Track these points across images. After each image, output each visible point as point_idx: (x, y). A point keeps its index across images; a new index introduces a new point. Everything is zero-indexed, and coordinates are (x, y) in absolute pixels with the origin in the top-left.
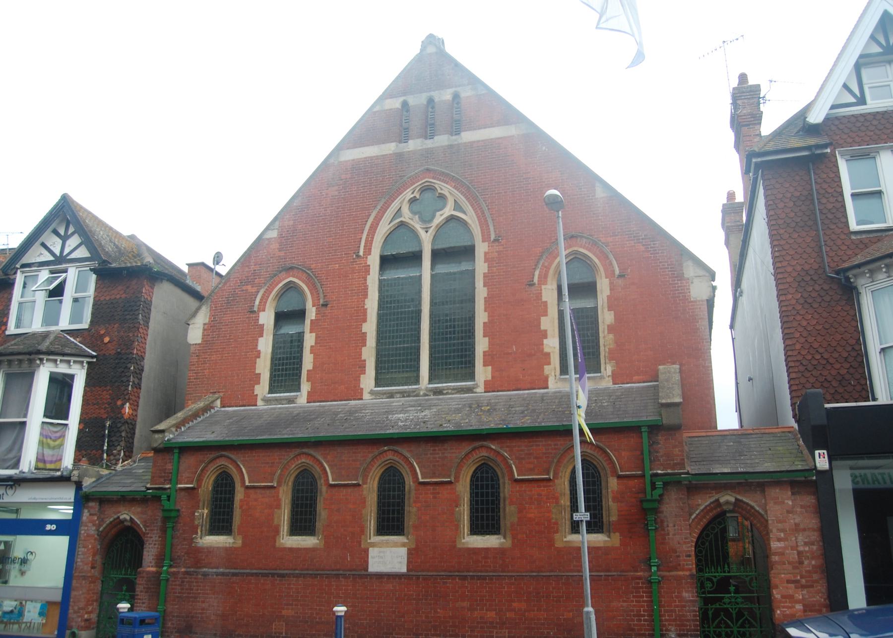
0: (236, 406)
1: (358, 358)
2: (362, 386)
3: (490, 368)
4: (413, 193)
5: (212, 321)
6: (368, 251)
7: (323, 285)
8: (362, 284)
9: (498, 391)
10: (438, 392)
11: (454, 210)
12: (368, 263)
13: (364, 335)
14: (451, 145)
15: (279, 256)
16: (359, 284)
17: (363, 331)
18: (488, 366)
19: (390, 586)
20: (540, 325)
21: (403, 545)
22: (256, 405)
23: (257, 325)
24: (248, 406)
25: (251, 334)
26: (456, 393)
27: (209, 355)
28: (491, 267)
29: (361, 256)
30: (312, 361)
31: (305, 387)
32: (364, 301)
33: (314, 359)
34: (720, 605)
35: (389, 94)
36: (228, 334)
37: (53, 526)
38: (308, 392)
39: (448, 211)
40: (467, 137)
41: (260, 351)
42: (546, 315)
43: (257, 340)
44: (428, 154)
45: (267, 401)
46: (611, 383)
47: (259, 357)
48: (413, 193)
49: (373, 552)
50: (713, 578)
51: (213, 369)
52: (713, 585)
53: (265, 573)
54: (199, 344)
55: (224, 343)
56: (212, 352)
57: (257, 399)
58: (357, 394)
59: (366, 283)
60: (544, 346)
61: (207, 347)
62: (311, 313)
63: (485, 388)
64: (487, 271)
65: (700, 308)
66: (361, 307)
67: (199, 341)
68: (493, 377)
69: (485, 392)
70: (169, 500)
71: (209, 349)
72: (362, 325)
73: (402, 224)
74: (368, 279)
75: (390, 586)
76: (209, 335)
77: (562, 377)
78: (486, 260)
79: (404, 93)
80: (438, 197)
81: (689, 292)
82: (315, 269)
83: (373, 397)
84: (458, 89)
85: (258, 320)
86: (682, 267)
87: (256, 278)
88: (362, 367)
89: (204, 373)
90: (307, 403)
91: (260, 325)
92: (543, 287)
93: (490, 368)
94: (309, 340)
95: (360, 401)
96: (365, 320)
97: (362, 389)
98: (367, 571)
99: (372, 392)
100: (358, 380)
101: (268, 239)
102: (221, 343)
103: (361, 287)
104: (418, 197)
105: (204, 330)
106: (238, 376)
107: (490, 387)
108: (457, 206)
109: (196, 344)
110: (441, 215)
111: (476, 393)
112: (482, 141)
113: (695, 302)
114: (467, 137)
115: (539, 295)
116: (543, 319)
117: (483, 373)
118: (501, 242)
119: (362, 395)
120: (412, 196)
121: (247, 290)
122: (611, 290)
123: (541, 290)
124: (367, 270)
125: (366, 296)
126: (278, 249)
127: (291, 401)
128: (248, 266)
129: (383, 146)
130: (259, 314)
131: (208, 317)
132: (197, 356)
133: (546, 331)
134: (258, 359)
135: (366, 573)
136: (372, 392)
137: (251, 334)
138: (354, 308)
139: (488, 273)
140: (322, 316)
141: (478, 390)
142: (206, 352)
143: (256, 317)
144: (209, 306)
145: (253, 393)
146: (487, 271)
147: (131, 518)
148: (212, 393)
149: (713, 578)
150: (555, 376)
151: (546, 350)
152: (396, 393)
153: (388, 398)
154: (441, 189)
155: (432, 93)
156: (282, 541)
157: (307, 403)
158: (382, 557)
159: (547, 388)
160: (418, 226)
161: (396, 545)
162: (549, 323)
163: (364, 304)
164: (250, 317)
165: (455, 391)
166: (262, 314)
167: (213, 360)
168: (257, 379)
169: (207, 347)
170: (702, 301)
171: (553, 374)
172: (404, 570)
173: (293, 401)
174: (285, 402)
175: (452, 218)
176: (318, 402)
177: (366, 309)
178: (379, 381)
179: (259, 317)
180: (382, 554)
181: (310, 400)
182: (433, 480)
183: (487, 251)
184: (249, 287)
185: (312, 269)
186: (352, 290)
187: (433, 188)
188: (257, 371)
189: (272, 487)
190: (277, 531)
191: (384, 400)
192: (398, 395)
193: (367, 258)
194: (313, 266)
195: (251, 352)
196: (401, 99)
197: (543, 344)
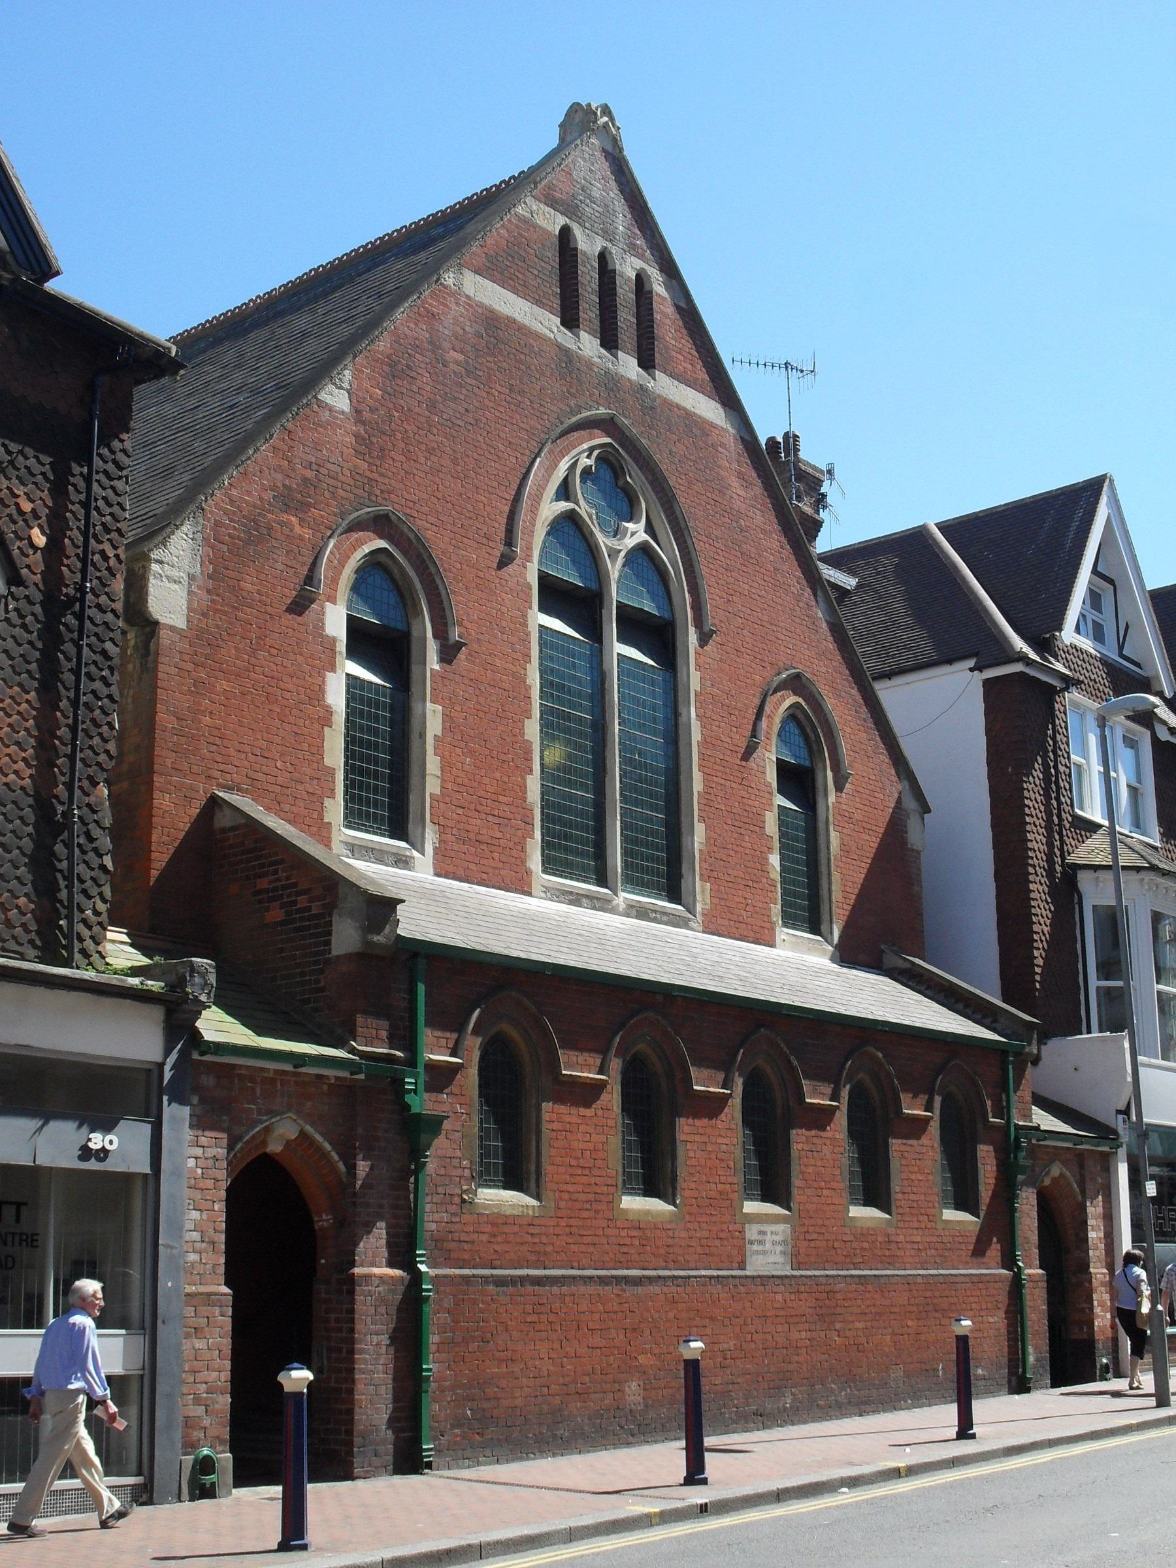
14: (641, 385)
23: (321, 636)
31: (431, 837)
37: (109, 1137)
38: (435, 849)
40: (664, 386)
41: (329, 706)
44: (612, 384)
49: (752, 1232)
53: (607, 1277)
67: (181, 623)
70: (415, 1091)
73: (571, 518)
92: (767, 754)
108: (650, 529)
113: (913, 850)
114: (664, 386)
117: (701, 892)
119: (530, 886)
120: (589, 462)
129: (538, 311)
147: (303, 1134)
161: (776, 1219)
162: (771, 825)
175: (643, 548)
177: (530, 687)
187: (615, 462)
196: (561, 220)
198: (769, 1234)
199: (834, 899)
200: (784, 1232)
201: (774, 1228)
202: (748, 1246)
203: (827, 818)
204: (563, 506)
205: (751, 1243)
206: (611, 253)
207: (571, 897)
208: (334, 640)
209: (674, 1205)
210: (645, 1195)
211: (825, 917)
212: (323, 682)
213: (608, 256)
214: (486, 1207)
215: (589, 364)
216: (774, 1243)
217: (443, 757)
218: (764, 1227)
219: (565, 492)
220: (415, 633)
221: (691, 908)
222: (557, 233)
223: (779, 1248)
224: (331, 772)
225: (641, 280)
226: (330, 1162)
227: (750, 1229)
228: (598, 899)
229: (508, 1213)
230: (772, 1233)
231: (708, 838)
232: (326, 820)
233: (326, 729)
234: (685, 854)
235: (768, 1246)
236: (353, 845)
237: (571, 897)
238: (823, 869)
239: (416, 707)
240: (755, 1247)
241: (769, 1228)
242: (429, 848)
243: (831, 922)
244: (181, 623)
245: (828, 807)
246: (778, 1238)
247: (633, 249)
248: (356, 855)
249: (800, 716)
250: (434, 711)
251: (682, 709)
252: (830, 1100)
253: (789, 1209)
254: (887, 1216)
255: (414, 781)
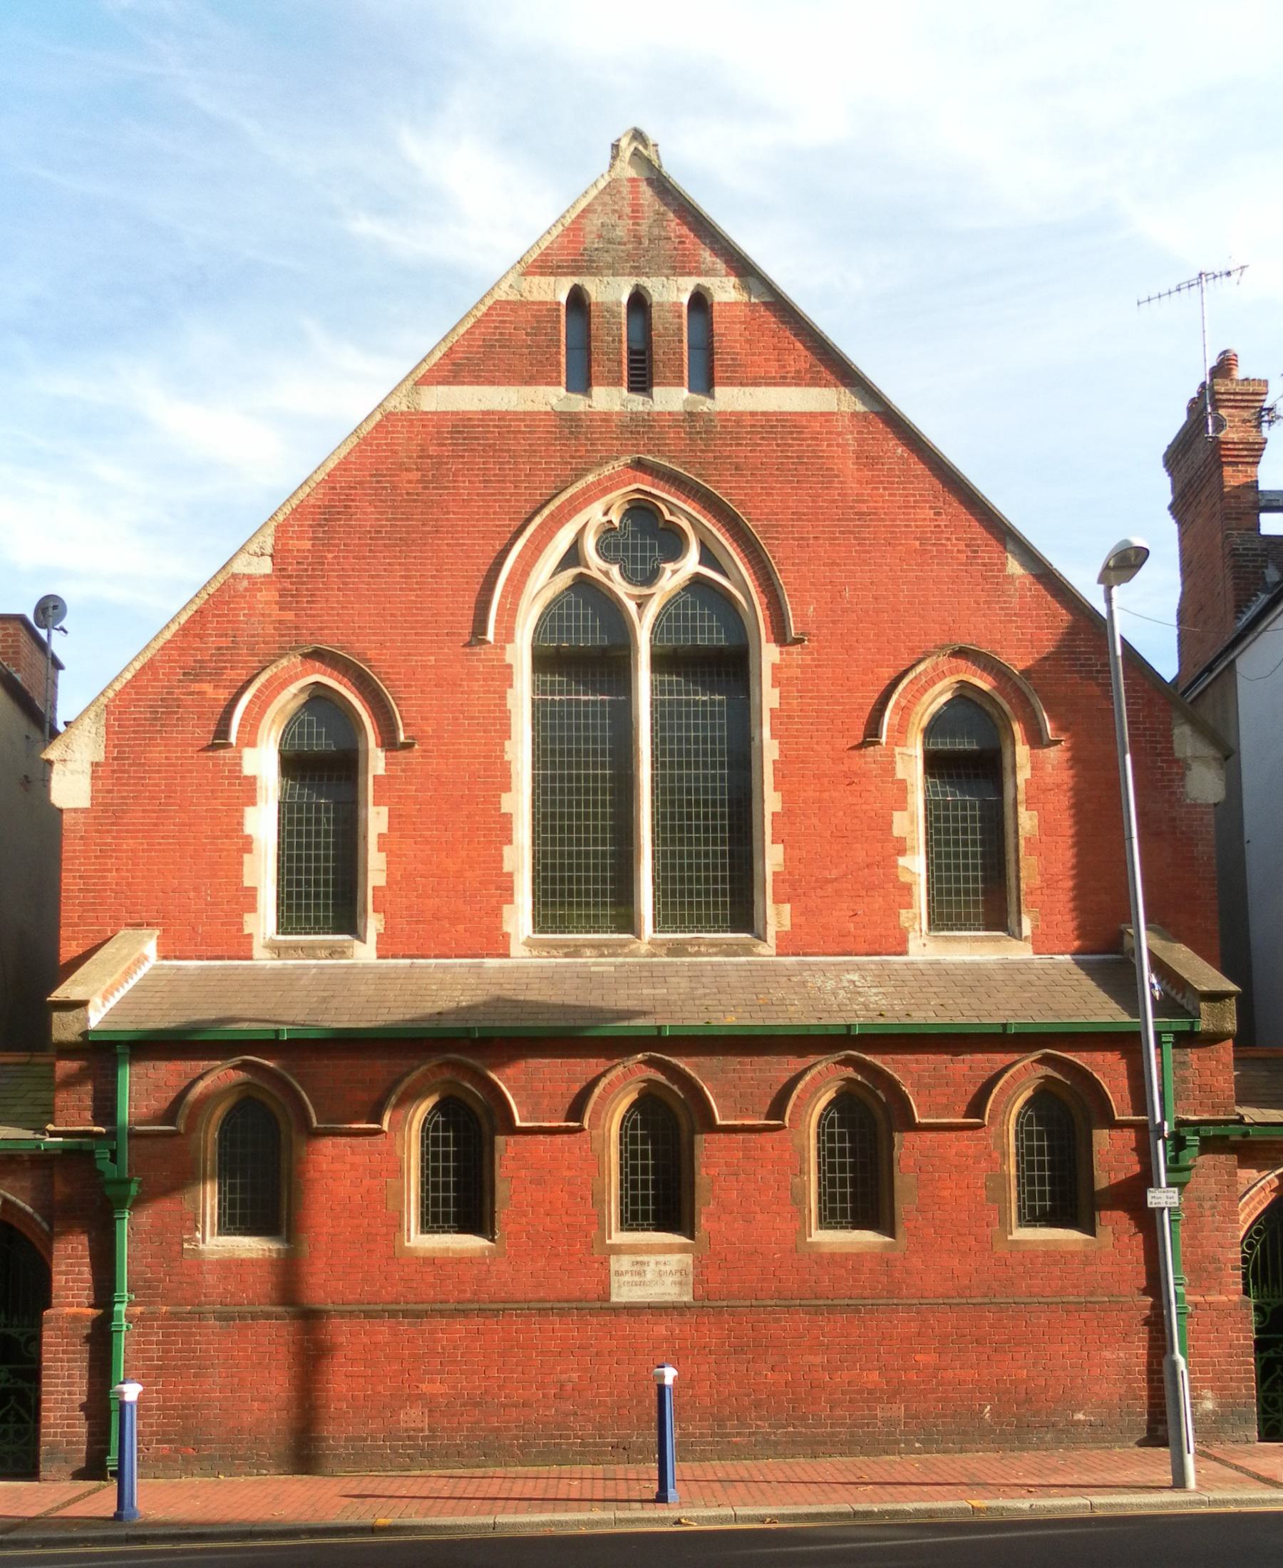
0: (199, 958)
1: (495, 869)
2: (507, 928)
3: (787, 907)
4: (606, 513)
5: (114, 759)
6: (507, 634)
7: (401, 698)
8: (495, 705)
9: (805, 955)
10: (677, 949)
11: (701, 563)
12: (509, 659)
13: (508, 818)
14: (690, 414)
15: (280, 622)
16: (489, 705)
17: (503, 811)
18: (783, 902)
19: (662, 1330)
20: (891, 828)
21: (683, 1249)
22: (250, 958)
23: (238, 778)
24: (230, 958)
25: (222, 798)
26: (716, 954)
27: (114, 838)
28: (787, 697)
29: (489, 643)
30: (385, 867)
31: (374, 924)
32: (503, 745)
33: (388, 863)
34: (1276, 1352)
35: (543, 265)
36: (162, 791)
38: (379, 935)
39: (690, 564)
41: (249, 837)
42: (904, 809)
43: (242, 812)
44: (640, 426)
45: (278, 950)
46: (1031, 952)
47: (249, 851)
48: (606, 513)
49: (620, 1264)
50: (1265, 1307)
51: (128, 871)
52: (1265, 1319)
54: (84, 811)
55: (154, 811)
56: (121, 831)
57: (250, 944)
58: (498, 945)
59: (505, 705)
60: (900, 870)
61: (108, 818)
62: (377, 762)
63: (777, 946)
64: (777, 706)
65: (1202, 819)
66: (497, 757)
67: (85, 803)
68: (792, 925)
69: (778, 955)
71: (113, 824)
72: (499, 796)
73: (583, 583)
74: (508, 695)
75: (662, 1330)
76: (109, 791)
77: (933, 933)
78: (776, 682)
79: (576, 270)
80: (662, 529)
81: (1183, 786)
82: (378, 661)
83: (535, 953)
84: (704, 281)
85: (240, 765)
86: (1172, 736)
87: (225, 668)
88: (506, 890)
89: (105, 877)
90: (379, 957)
91: (246, 777)
92: (897, 750)
93: (787, 907)
94: (376, 820)
95: (505, 960)
96: (507, 788)
97: (506, 936)
98: (608, 1300)
99: (530, 944)
100: (497, 913)
101: (249, 577)
102: (144, 811)
103: (494, 711)
104: (616, 522)
105: (94, 777)
106: (196, 889)
107: (787, 946)
108: (708, 558)
109: (75, 810)
110: (674, 572)
111: (759, 955)
112: (764, 414)
113: (1195, 806)
115: (889, 768)
116: (897, 816)
118: (807, 647)
119: (508, 948)
120: (605, 519)
121: (204, 693)
122: (1033, 769)
123: (893, 756)
124: (506, 674)
125: (506, 733)
126: (277, 603)
127: (335, 952)
128: (201, 637)
129: (528, 391)
130: (240, 752)
131: (103, 747)
132: (82, 838)
133: (902, 840)
134: (246, 857)
135: (605, 1305)
136: (530, 944)
137: (222, 798)
138: (478, 757)
139: (781, 710)
140: (403, 771)
141: (762, 949)
142: (108, 831)
143: (234, 758)
144: (103, 722)
145: (241, 930)
146: (777, 706)
148: (127, 925)
149: (1265, 1307)
150: (921, 931)
151: (904, 878)
152: (584, 946)
153: (567, 955)
154: (672, 513)
155: (645, 281)
156: (407, 1244)
157: (379, 957)
158: (639, 1274)
159: (904, 952)
160: (621, 588)
161: (668, 1249)
163: (503, 751)
164: (218, 758)
165: (714, 950)
166: (247, 753)
167: (127, 851)
168: (248, 899)
169: (108, 818)
170: (1208, 806)
171: (917, 927)
172: (687, 1298)
173: (344, 952)
174: (324, 953)
175: (697, 582)
176: (404, 957)
177: (510, 762)
178: (543, 921)
179: (241, 758)
180: (636, 1268)
181: (384, 953)
182: (746, 1122)
183: (778, 662)
184: (207, 688)
185: (369, 660)
186: (473, 718)
187: (650, 506)
188: (247, 883)
189: (378, 1132)
190: (397, 1224)
191: (559, 960)
192: (588, 952)
193: (503, 648)
194: (371, 654)
195: (227, 837)
197: (896, 866)
198: (652, 1265)
199: (1023, 886)
200: (680, 1260)
201: (661, 1258)
202: (614, 1278)
203: (1015, 799)
204: (573, 572)
205: (618, 1273)
206: (644, 288)
207: (566, 950)
208: (251, 782)
209: (492, 1240)
210: (457, 1232)
211: (1012, 908)
212: (242, 817)
213: (643, 292)
214: (213, 1253)
215: (606, 417)
216: (660, 1274)
217: (390, 854)
218: (640, 1258)
219: (573, 556)
220: (361, 748)
221: (761, 933)
222: (563, 298)
223: (669, 1280)
224: (251, 893)
225: (700, 302)
226: (38, 1224)
227: (618, 1261)
228: (606, 946)
229: (244, 1256)
230: (657, 1263)
231: (787, 859)
232: (247, 931)
233: (246, 857)
234: (757, 879)
235: (649, 1276)
236: (279, 948)
237: (566, 950)
238: (1011, 856)
239: (361, 813)
240: (627, 1278)
241: (652, 1259)
242: (371, 936)
243: (1019, 913)
244: (85, 803)
245: (1016, 786)
246: (668, 1268)
247: (681, 267)
248: (282, 956)
249: (970, 694)
250: (378, 813)
251: (755, 733)
252: (766, 1119)
253: (692, 1237)
254: (888, 1239)
255: (360, 878)
